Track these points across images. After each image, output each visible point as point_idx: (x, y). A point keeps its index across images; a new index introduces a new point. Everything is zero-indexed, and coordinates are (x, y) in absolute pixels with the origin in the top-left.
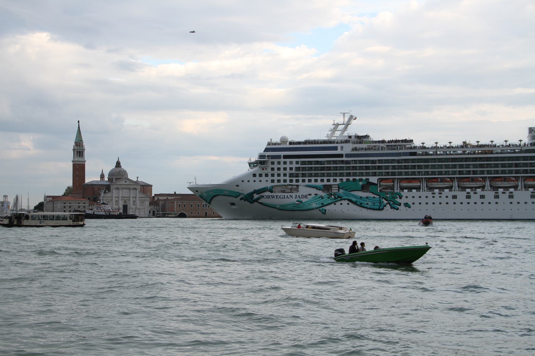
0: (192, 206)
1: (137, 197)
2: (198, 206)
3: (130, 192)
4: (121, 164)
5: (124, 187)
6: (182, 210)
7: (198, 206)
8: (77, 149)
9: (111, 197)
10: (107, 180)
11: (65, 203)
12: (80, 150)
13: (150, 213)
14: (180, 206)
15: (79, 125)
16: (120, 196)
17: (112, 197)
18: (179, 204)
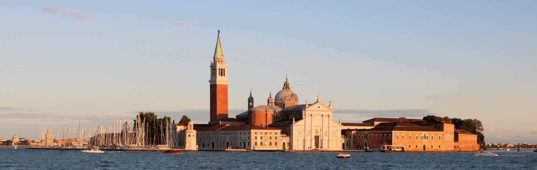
11: (256, 133)
12: (222, 68)
15: (218, 36)
18: (397, 135)
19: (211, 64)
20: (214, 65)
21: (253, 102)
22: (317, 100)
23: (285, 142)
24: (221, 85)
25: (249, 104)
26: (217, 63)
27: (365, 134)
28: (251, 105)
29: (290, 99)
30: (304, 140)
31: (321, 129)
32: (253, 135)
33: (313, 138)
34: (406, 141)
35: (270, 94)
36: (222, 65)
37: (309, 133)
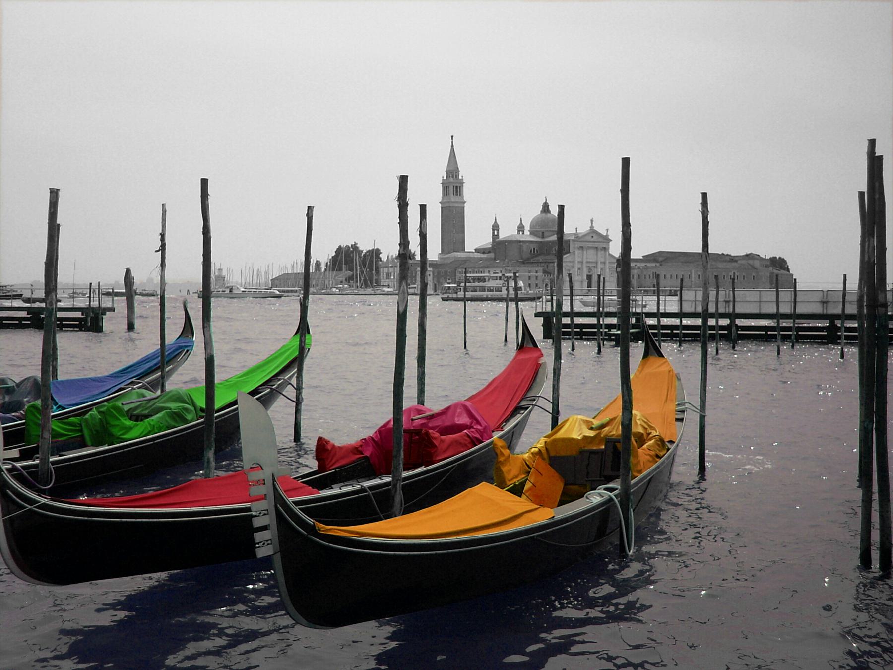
1: (607, 262)
3: (597, 254)
4: (550, 209)
5: (590, 245)
8: (453, 183)
9: (570, 262)
10: (529, 233)
12: (457, 185)
14: (699, 278)
15: (452, 142)
16: (585, 261)
17: (574, 262)
18: (699, 273)
19: (443, 180)
20: (446, 181)
21: (498, 230)
22: (591, 227)
24: (456, 207)
25: (494, 233)
26: (451, 178)
27: (653, 273)
28: (496, 233)
33: (585, 278)
35: (521, 219)
37: (579, 271)
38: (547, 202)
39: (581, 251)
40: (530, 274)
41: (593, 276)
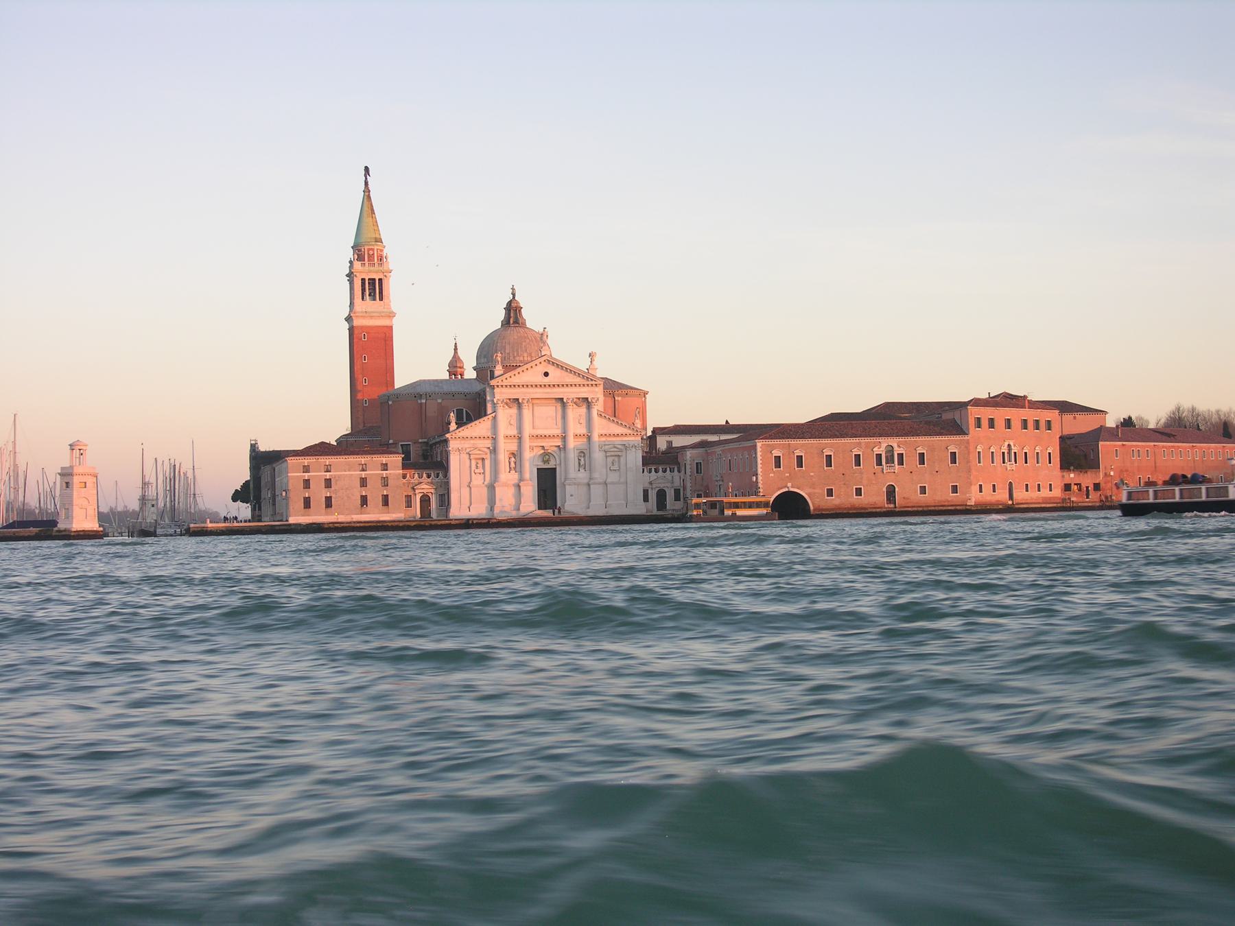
0: (829, 464)
2: (858, 463)
3: (564, 417)
5: (539, 393)
6: (790, 479)
7: (858, 463)
11: (306, 469)
13: (646, 499)
14: (778, 465)
15: (366, 183)
18: (776, 453)
23: (430, 495)
29: (509, 354)
30: (491, 488)
31: (561, 446)
32: (299, 474)
33: (530, 474)
34: (812, 474)
36: (372, 268)
37: (513, 459)
38: (516, 298)
39: (514, 411)
40: (363, 474)
41: (558, 469)
